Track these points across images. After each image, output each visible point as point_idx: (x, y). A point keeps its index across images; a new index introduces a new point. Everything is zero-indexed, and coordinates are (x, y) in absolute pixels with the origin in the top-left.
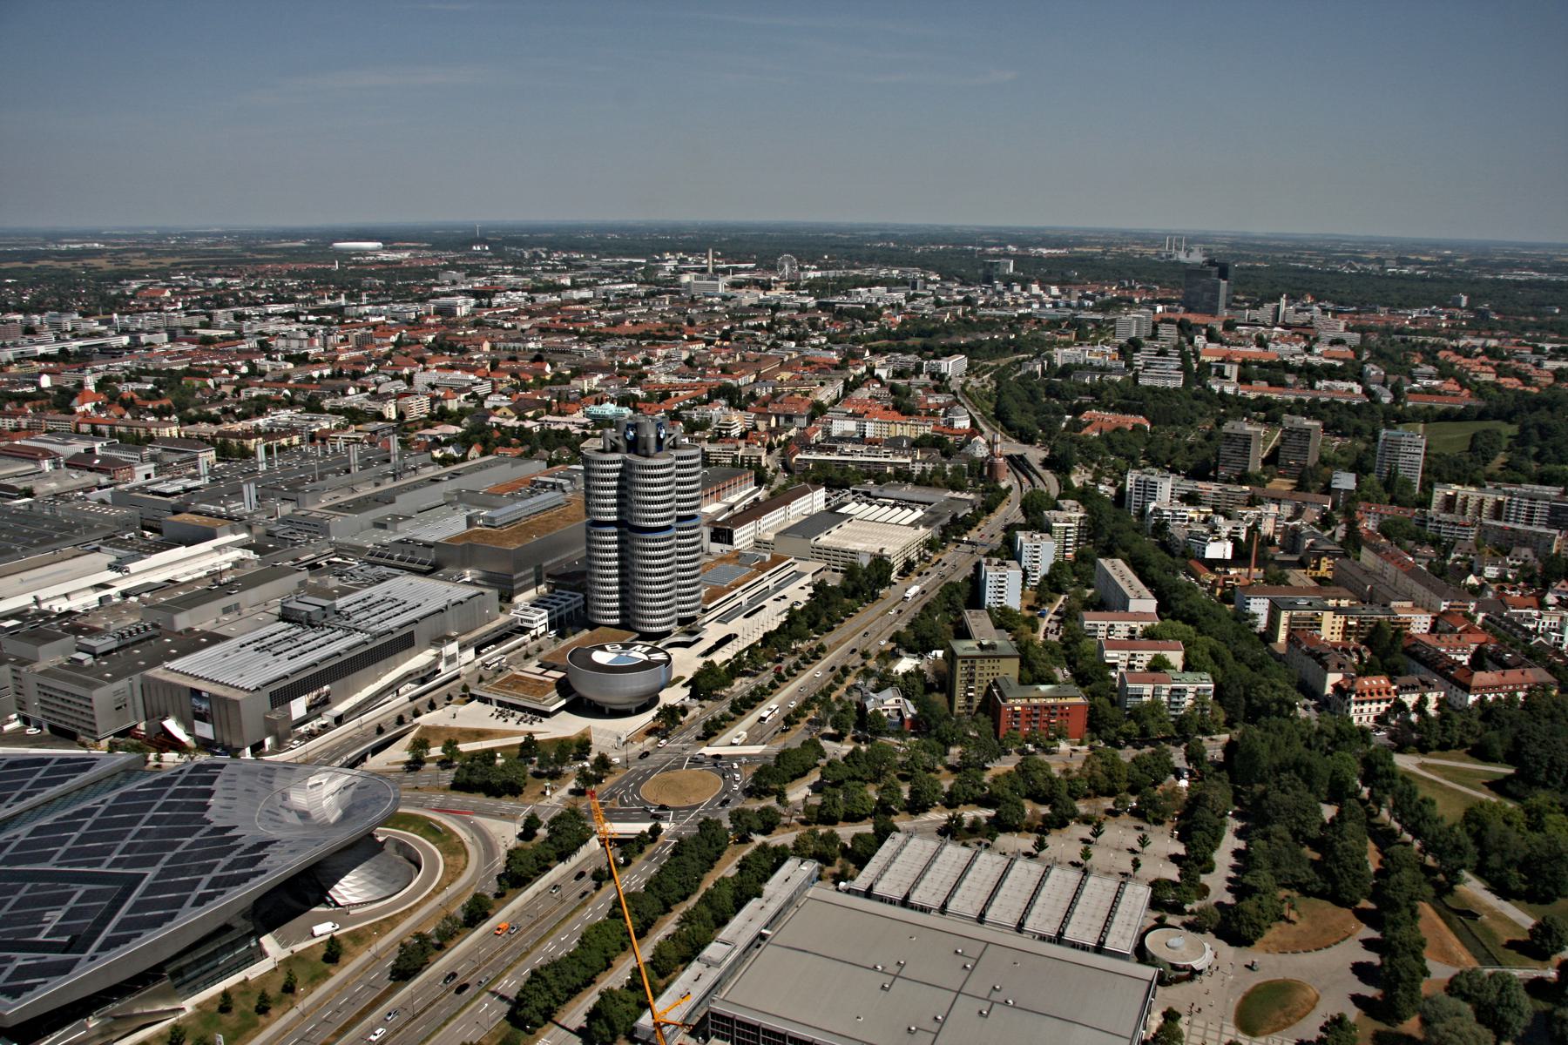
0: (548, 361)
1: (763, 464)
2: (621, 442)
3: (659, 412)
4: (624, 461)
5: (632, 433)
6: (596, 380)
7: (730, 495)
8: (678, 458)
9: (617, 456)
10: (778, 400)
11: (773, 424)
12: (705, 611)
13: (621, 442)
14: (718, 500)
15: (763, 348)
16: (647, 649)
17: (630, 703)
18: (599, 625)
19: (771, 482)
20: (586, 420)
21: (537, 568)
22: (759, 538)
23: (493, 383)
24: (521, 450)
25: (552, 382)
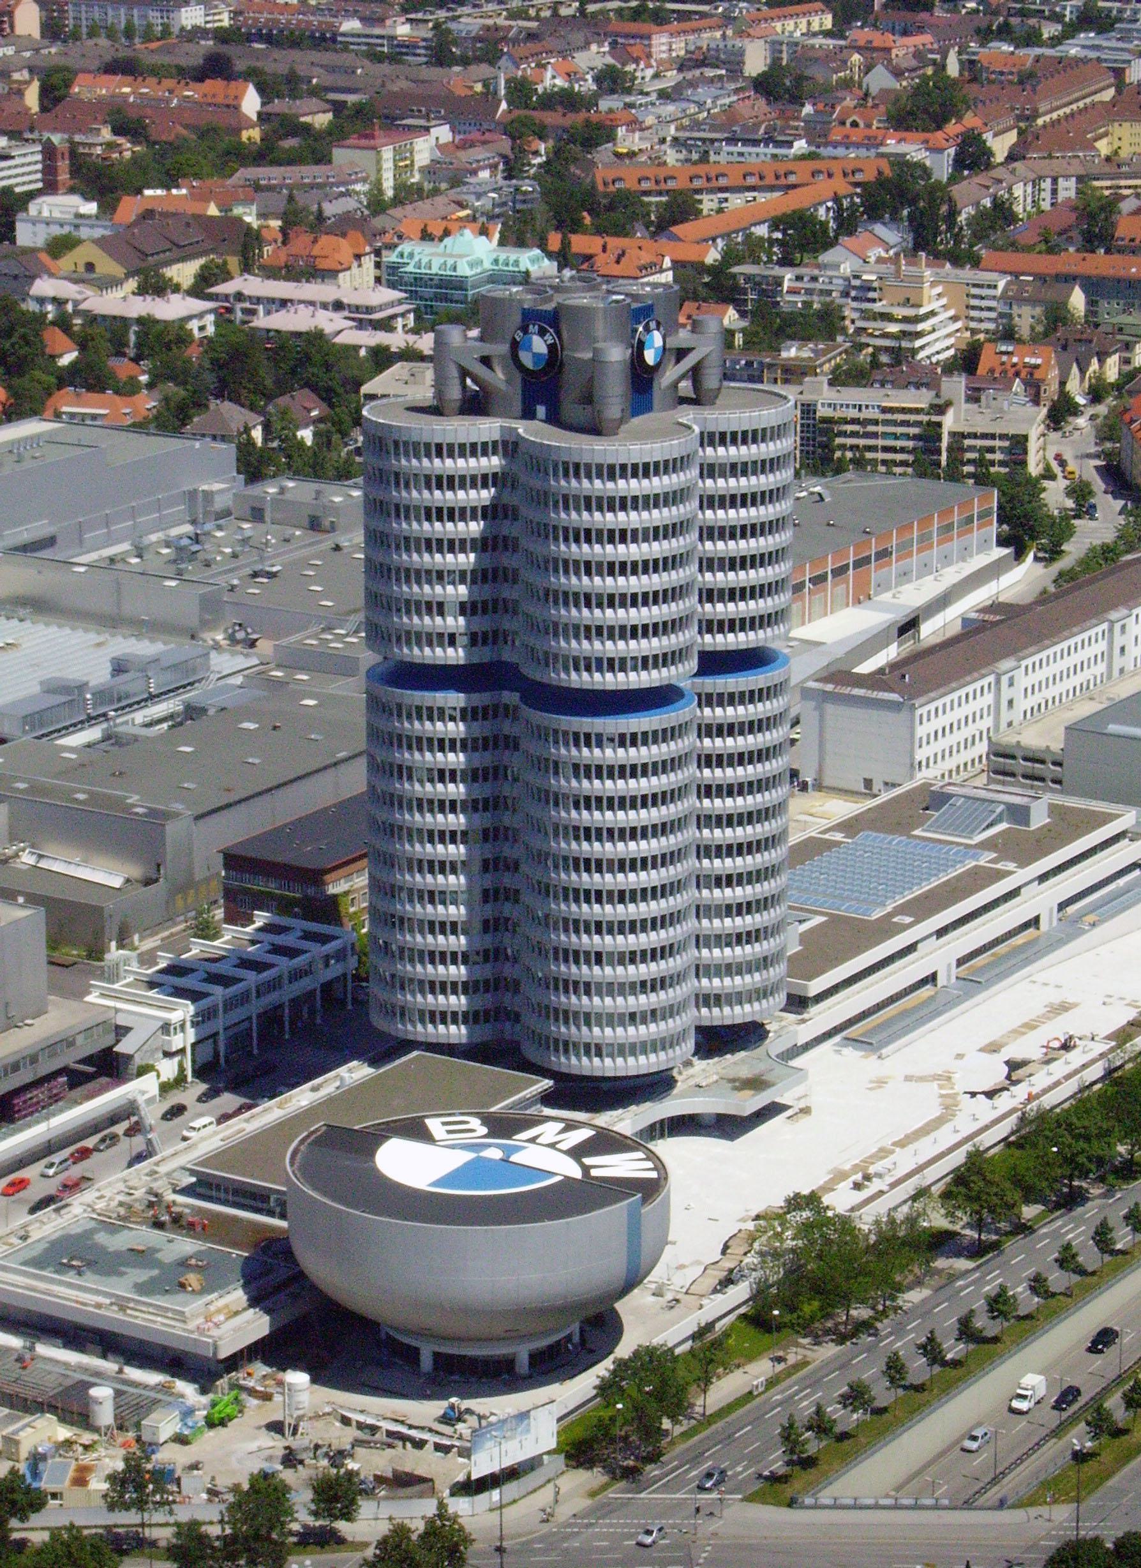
0: (252, 75)
1: (1034, 468)
2: (498, 377)
3: (653, 267)
4: (510, 447)
5: (539, 345)
6: (424, 150)
7: (905, 576)
8: (710, 439)
9: (487, 428)
12: (798, 1003)
13: (498, 377)
14: (861, 597)
15: (1049, 30)
16: (582, 1135)
17: (512, 1336)
18: (407, 1045)
22: (1008, 738)
23: (49, 152)
25: (263, 155)
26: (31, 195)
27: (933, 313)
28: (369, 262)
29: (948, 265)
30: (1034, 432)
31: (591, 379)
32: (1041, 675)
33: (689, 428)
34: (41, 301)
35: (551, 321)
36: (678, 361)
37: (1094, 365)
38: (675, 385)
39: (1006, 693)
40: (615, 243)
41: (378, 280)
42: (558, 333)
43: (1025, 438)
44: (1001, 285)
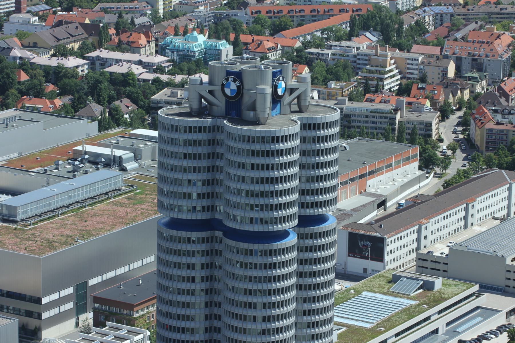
1: (434, 137)
10: (459, 35)
11: (451, 73)
14: (363, 192)
19: (446, 163)
20: (159, 59)
21: (77, 290)
24: (58, 102)
26: (9, 14)
27: (391, 71)
28: (153, 45)
29: (397, 50)
30: (435, 121)
31: (255, 101)
32: (438, 226)
33: (296, 122)
34: (15, 58)
35: (238, 76)
36: (291, 94)
37: (459, 94)
38: (290, 104)
39: (424, 233)
40: (256, 38)
41: (157, 52)
42: (242, 82)
43: (431, 124)
44: (420, 59)
